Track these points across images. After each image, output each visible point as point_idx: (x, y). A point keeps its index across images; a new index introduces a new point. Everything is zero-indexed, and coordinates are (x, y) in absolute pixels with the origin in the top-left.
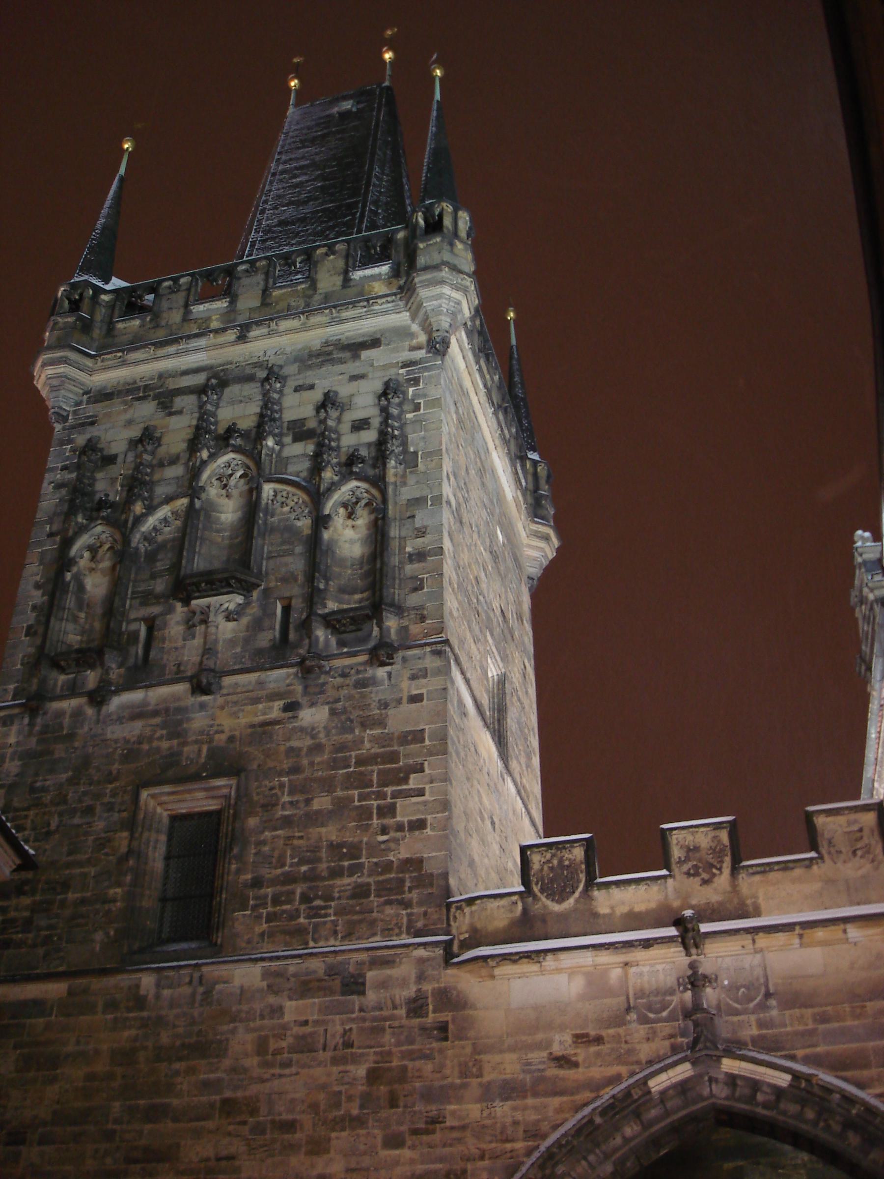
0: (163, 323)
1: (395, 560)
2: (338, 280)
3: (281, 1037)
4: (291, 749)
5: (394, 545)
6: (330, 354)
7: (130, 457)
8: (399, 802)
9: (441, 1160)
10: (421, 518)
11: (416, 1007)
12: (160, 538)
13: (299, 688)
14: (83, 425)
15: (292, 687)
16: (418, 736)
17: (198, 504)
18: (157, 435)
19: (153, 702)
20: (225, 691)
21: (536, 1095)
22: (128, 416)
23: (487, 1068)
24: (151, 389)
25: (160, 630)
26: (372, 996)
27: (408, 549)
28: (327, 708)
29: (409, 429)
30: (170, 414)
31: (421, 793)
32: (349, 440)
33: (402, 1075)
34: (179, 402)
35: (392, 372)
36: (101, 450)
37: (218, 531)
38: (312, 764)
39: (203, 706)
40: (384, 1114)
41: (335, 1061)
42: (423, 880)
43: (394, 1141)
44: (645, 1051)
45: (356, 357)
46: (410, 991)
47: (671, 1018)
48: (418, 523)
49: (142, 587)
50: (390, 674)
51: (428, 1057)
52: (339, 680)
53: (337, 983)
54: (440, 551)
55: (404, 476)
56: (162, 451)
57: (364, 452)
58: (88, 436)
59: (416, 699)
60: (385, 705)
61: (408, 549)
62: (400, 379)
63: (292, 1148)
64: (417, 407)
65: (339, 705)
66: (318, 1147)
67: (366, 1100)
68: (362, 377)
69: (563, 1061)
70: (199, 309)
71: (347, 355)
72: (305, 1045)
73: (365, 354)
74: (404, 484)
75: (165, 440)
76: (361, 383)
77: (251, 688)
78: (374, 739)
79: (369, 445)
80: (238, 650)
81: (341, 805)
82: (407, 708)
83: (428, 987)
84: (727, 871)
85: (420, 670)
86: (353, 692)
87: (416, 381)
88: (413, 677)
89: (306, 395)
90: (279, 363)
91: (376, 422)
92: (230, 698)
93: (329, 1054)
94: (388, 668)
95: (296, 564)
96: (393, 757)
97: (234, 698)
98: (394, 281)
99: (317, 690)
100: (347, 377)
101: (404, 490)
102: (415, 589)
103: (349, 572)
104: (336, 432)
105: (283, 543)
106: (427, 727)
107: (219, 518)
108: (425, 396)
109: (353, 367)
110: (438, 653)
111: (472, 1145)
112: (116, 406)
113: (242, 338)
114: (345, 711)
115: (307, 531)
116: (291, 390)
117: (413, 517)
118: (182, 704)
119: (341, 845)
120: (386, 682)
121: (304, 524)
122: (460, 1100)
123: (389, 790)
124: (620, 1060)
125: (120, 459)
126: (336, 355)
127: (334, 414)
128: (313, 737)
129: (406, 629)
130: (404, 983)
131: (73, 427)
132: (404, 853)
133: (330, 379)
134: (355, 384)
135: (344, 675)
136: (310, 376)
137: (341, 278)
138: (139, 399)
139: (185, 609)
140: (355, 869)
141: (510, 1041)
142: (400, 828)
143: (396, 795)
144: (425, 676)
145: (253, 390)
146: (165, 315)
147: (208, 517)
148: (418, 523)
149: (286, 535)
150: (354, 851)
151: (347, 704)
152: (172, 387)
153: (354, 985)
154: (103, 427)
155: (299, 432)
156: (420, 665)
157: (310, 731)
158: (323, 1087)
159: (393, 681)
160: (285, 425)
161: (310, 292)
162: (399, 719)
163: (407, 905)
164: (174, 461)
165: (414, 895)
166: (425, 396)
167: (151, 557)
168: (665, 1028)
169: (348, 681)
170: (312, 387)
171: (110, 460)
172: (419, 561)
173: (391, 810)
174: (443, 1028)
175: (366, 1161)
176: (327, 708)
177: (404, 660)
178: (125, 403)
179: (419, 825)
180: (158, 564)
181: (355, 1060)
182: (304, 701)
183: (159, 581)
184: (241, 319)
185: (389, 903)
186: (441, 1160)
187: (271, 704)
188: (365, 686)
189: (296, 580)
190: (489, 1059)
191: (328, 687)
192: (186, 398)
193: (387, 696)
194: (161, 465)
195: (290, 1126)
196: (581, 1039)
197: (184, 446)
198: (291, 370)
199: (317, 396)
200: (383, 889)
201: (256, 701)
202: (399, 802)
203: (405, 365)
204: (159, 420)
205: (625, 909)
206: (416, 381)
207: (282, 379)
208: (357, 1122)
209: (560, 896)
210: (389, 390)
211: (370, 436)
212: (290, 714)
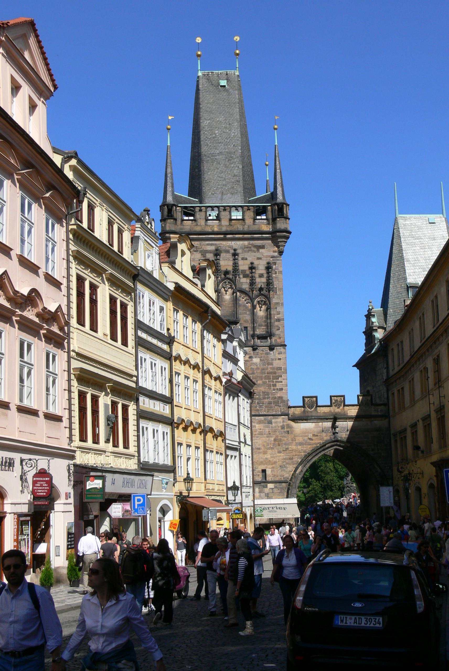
0: (199, 224)
1: (273, 321)
3: (256, 432)
4: (252, 368)
5: (272, 316)
6: (251, 248)
8: (277, 384)
9: (288, 456)
10: (279, 309)
11: (283, 427)
13: (252, 352)
16: (280, 369)
21: (306, 445)
23: (297, 440)
24: (199, 248)
26: (274, 425)
27: (276, 318)
29: (274, 280)
31: (282, 382)
33: (280, 440)
38: (257, 372)
40: (278, 447)
41: (267, 437)
42: (283, 401)
43: (279, 452)
44: (325, 438)
45: (258, 251)
46: (282, 424)
47: (330, 433)
51: (286, 437)
53: (266, 422)
54: (283, 320)
55: (274, 295)
57: (263, 286)
59: (279, 359)
60: (273, 360)
61: (276, 318)
63: (260, 453)
64: (276, 273)
65: (262, 358)
66: (265, 453)
67: (274, 444)
69: (310, 439)
71: (255, 249)
72: (261, 434)
73: (261, 250)
74: (274, 297)
76: (260, 261)
78: (271, 368)
79: (264, 283)
81: (264, 383)
83: (285, 424)
84: (342, 406)
86: (266, 356)
87: (275, 264)
88: (279, 354)
89: (245, 261)
90: (236, 248)
91: (265, 275)
93: (266, 435)
95: (248, 317)
96: (275, 373)
98: (268, 226)
100: (256, 257)
101: (273, 299)
105: (243, 310)
108: (278, 269)
109: (258, 255)
110: (284, 348)
111: (294, 453)
115: (250, 308)
117: (276, 308)
119: (265, 392)
122: (291, 445)
123: (275, 380)
124: (321, 440)
126: (253, 249)
127: (254, 271)
128: (257, 366)
130: (280, 422)
132: (279, 395)
133: (251, 257)
134: (258, 261)
136: (246, 255)
140: (268, 398)
141: (301, 435)
142: (277, 389)
143: (276, 382)
145: (229, 256)
146: (199, 221)
149: (244, 308)
150: (268, 394)
152: (205, 249)
153: (270, 422)
155: (245, 276)
156: (280, 350)
157: (255, 364)
158: (265, 442)
161: (243, 224)
162: (276, 364)
163: (280, 406)
165: (281, 405)
166: (278, 269)
168: (329, 434)
170: (246, 259)
173: (275, 385)
174: (288, 432)
175: (275, 455)
179: (282, 389)
181: (271, 437)
182: (254, 356)
184: (224, 229)
185: (276, 406)
186: (288, 456)
188: (268, 354)
190: (297, 438)
191: (259, 353)
193: (273, 357)
195: (259, 449)
196: (314, 435)
198: (239, 251)
199: (248, 262)
200: (275, 403)
202: (277, 384)
203: (273, 257)
205: (323, 411)
206: (275, 264)
208: (272, 448)
209: (311, 407)
210: (268, 268)
211: (264, 280)
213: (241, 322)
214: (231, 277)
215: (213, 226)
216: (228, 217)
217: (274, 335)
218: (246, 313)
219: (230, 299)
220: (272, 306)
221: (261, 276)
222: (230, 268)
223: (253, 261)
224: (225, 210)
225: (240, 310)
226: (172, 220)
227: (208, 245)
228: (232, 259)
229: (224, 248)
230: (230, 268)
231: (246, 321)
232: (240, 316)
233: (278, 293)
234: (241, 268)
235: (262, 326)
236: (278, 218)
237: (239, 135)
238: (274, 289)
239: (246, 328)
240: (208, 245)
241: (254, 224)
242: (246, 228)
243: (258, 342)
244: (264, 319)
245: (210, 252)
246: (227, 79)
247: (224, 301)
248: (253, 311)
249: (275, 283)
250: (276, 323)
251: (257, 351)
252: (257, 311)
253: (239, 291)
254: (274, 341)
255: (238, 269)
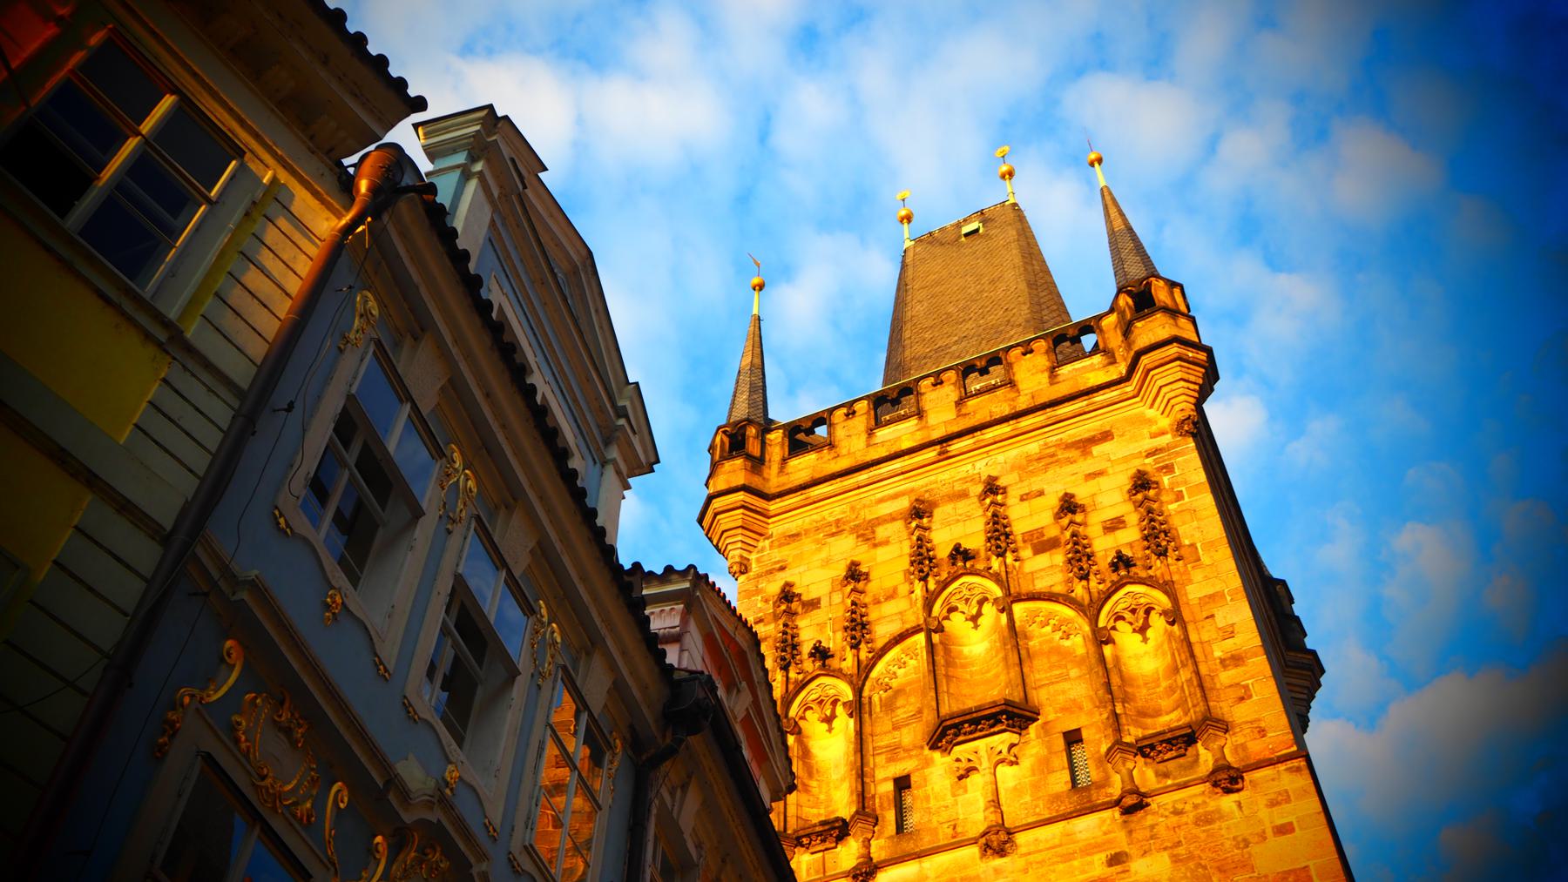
0: (844, 451)
1: (1203, 670)
2: (1044, 378)
5: (1197, 650)
6: (1053, 456)
7: (837, 598)
12: (894, 683)
13: (1121, 835)
14: (770, 572)
15: (1112, 836)
17: (936, 638)
18: (864, 569)
19: (932, 874)
20: (1023, 850)
22: (823, 555)
25: (918, 788)
28: (1165, 856)
29: (1175, 521)
30: (875, 546)
32: (1104, 546)
34: (882, 532)
35: (1137, 464)
36: (799, 595)
37: (963, 666)
39: (997, 871)
48: (1221, 620)
49: (884, 741)
50: (1239, 805)
52: (1174, 819)
56: (873, 587)
57: (1127, 552)
58: (782, 583)
60: (1247, 843)
61: (1218, 654)
62: (1148, 469)
64: (1179, 496)
65: (1181, 850)
68: (1100, 473)
70: (883, 434)
71: (1074, 453)
73: (1096, 450)
74: (1190, 582)
75: (872, 577)
76: (1101, 480)
77: (1057, 841)
79: (1131, 545)
80: (1028, 798)
82: (1274, 842)
85: (1280, 793)
86: (1196, 831)
87: (1169, 469)
88: (1273, 804)
90: (994, 474)
91: (1133, 518)
92: (1031, 858)
94: (1234, 797)
97: (1038, 857)
99: (1148, 833)
100: (1081, 476)
101: (1189, 588)
102: (1242, 699)
103: (1144, 691)
104: (1086, 537)
105: (1051, 668)
106: (1311, 863)
107: (961, 652)
108: (1185, 483)
109: (1087, 465)
112: (807, 545)
113: (944, 456)
114: (1191, 857)
115: (1081, 651)
116: (1017, 500)
117: (1212, 616)
118: (971, 872)
120: (1237, 813)
121: (1078, 643)
125: (824, 603)
126: (1062, 455)
127: (1079, 518)
129: (1243, 746)
131: (759, 576)
134: (1092, 483)
135: (1177, 813)
136: (1035, 484)
137: (1046, 374)
138: (833, 535)
139: (948, 759)
144: (1288, 800)
147: (947, 651)
148: (1221, 620)
149: (1054, 659)
151: (1192, 848)
152: (869, 517)
154: (797, 571)
155: (1043, 545)
156: (1275, 787)
159: (1246, 812)
160: (1019, 538)
161: (1013, 395)
164: (892, 595)
166: (1185, 483)
167: (889, 706)
169: (1184, 819)
170: (1041, 493)
171: (814, 604)
172: (1236, 666)
176: (1165, 856)
177: (1254, 784)
178: (817, 542)
180: (899, 712)
183: (905, 730)
184: (937, 434)
187: (1089, 859)
188: (1209, 821)
189: (1081, 708)
192: (889, 526)
193: (1244, 831)
194: (877, 602)
197: (900, 577)
199: (1052, 501)
201: (1067, 858)
204: (862, 554)
206: (1169, 469)
207: (1004, 491)
212: (1118, 868)
213: (1048, 714)
214: (980, 566)
215: (898, 439)
216: (954, 396)
217: (1226, 727)
218: (1067, 678)
219: (988, 651)
220: (1186, 615)
221: (1114, 525)
222: (975, 539)
223: (1070, 491)
224: (938, 383)
225: (1039, 672)
226: (739, 462)
227: (881, 501)
228: (980, 512)
229: (945, 490)
230: (975, 539)
231: (1071, 707)
232: (1040, 696)
233: (1205, 559)
234: (1019, 527)
235: (1158, 713)
236: (1139, 319)
237: (1023, 286)
238: (1183, 552)
239: (1073, 738)
240: (881, 501)
241: (1051, 384)
242: (1023, 403)
243: (1146, 774)
244: (1164, 684)
245: (892, 518)
246: (984, 222)
247: (963, 666)
248: (1102, 659)
249: (1181, 531)
250: (1225, 677)
251: (1150, 820)
252: (1117, 659)
253: (1018, 599)
254: (1235, 749)
255: (1011, 533)
